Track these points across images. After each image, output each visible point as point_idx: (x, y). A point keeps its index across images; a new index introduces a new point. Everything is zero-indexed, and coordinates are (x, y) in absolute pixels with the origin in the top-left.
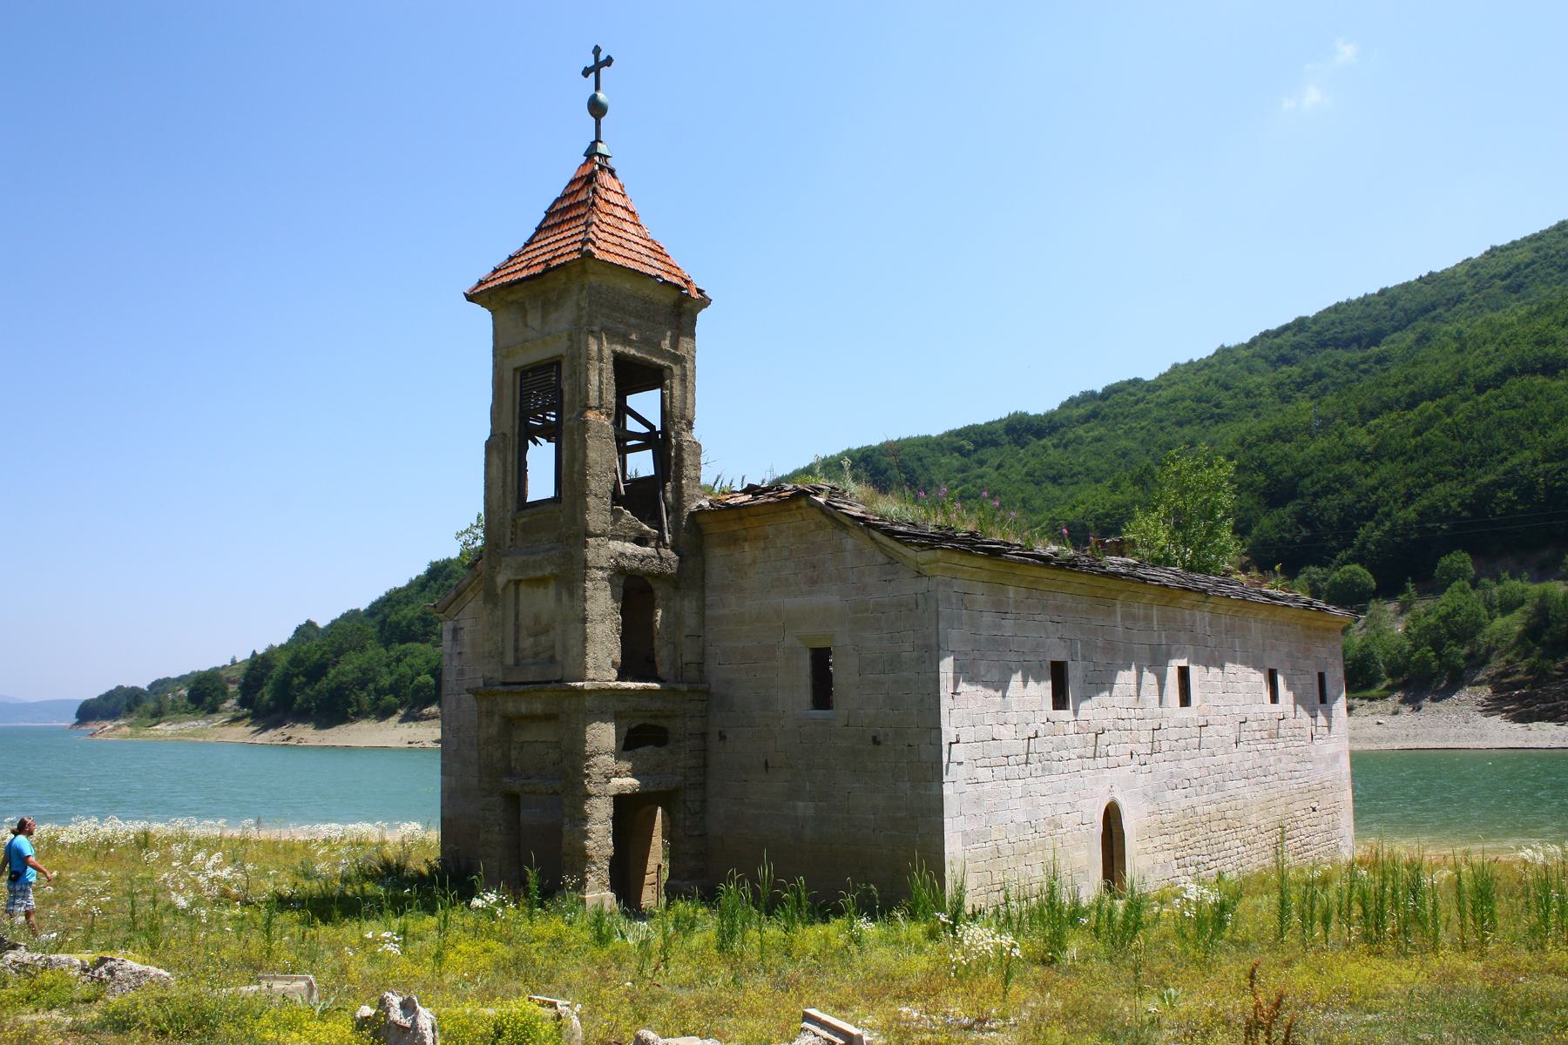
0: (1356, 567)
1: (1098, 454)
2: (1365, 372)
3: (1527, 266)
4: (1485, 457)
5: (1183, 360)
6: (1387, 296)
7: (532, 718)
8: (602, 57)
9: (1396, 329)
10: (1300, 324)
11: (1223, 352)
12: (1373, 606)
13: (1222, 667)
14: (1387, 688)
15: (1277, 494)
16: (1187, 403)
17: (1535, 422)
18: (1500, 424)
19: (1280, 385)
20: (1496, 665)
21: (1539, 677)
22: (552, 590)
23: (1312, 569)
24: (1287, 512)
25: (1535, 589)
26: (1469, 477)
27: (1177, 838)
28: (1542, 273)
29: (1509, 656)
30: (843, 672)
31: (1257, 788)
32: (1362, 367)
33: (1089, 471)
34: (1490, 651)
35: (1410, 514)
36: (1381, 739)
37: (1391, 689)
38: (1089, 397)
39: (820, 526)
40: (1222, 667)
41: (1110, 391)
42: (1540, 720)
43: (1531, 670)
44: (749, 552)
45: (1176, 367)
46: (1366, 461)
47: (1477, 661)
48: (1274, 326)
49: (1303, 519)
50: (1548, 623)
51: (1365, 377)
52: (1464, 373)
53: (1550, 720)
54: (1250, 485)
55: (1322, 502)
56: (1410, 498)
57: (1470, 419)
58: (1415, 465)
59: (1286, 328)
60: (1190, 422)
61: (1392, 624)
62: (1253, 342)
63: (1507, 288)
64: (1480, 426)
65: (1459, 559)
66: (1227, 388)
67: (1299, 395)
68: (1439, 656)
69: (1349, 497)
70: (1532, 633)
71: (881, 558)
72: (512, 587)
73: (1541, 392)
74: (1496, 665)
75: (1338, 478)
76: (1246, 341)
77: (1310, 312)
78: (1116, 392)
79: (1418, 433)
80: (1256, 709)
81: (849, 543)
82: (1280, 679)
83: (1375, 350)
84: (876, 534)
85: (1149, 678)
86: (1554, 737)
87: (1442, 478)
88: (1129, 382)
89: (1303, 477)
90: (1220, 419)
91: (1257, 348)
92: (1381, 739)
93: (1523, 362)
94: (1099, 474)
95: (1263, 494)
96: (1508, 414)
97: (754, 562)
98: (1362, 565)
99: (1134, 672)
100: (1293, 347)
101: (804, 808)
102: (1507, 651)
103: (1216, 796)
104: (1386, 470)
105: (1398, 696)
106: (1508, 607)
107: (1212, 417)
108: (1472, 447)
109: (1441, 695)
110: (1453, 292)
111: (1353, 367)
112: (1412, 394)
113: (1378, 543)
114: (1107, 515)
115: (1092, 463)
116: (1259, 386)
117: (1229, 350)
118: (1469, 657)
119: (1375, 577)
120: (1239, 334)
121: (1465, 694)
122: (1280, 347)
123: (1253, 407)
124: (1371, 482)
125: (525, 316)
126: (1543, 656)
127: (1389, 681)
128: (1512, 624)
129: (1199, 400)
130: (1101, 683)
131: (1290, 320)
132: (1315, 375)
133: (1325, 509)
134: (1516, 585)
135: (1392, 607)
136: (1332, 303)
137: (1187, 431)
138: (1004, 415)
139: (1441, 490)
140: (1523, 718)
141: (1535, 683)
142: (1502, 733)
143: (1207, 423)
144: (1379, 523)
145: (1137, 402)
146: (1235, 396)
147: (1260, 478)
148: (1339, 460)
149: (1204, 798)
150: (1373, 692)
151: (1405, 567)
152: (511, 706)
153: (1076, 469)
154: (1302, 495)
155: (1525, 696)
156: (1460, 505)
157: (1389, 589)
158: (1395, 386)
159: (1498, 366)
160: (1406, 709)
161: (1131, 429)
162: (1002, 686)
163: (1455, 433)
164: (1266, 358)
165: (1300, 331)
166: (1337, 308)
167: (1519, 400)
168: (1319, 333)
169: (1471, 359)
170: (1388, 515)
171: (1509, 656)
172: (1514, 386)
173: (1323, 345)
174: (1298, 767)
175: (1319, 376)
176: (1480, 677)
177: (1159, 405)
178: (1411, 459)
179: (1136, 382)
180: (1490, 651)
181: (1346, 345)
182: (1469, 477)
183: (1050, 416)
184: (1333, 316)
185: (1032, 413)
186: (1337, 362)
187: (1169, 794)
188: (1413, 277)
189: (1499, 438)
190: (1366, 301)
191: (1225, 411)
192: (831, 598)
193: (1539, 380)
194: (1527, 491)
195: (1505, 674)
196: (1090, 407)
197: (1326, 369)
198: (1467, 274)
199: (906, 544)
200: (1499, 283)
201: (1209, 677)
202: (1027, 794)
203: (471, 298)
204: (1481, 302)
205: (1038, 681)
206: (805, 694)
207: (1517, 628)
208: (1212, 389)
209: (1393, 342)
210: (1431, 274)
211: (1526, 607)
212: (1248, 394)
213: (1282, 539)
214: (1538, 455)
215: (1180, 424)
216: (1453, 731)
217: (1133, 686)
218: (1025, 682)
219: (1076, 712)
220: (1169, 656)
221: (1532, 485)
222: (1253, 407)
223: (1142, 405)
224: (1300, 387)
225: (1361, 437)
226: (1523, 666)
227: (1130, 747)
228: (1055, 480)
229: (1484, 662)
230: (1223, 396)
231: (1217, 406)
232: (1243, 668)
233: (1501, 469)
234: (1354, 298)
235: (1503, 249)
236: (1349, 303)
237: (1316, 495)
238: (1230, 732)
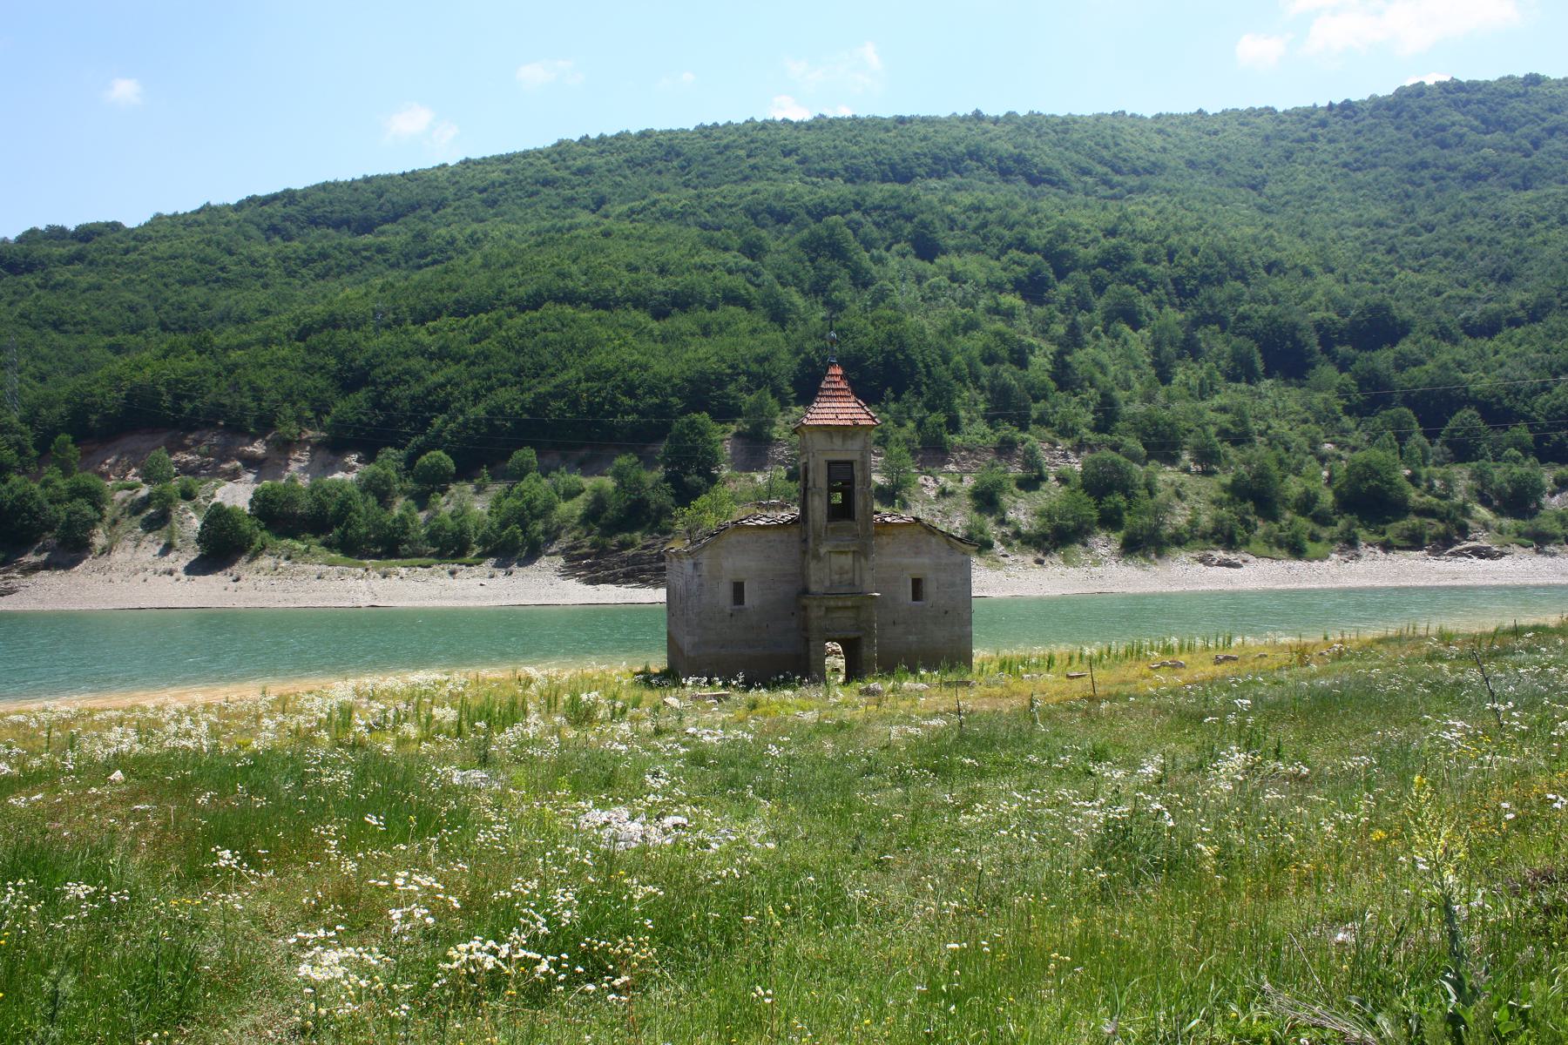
0: (440, 453)
1: (100, 304)
2: (369, 259)
3: (502, 184)
4: (539, 370)
5: (168, 211)
6: (376, 186)
7: (838, 608)
9: (385, 221)
10: (289, 196)
12: (453, 488)
14: (479, 556)
15: (351, 380)
16: (190, 262)
17: (573, 346)
18: (546, 345)
19: (286, 259)
20: (565, 540)
21: (601, 551)
22: (850, 556)
23: (390, 450)
24: (361, 395)
25: (589, 483)
26: (526, 385)
28: (513, 195)
29: (576, 533)
30: (930, 588)
32: (365, 254)
33: (95, 322)
34: (560, 528)
35: (478, 411)
36: (487, 598)
37: (483, 556)
38: (57, 234)
41: (87, 234)
42: (604, 582)
43: (594, 545)
44: (885, 539)
45: (159, 218)
46: (431, 359)
47: (552, 535)
48: (262, 192)
49: (376, 404)
50: (605, 509)
51: (368, 264)
52: (501, 291)
53: (612, 582)
54: (322, 368)
55: (394, 392)
56: (477, 396)
57: (521, 336)
58: (476, 370)
59: (274, 198)
60: (194, 282)
61: (474, 503)
62: (239, 206)
63: (484, 201)
64: (529, 343)
65: (527, 454)
66: (231, 253)
67: (304, 271)
68: (524, 533)
69: (417, 389)
70: (593, 515)
73: (573, 321)
74: (565, 540)
75: (407, 372)
76: (233, 202)
77: (298, 184)
78: (100, 234)
79: (474, 341)
81: (934, 540)
83: (368, 239)
86: (617, 596)
87: (504, 384)
88: (107, 225)
89: (373, 367)
90: (228, 283)
91: (246, 213)
92: (487, 598)
93: (549, 290)
94: (109, 327)
95: (334, 377)
96: (552, 336)
98: (447, 452)
100: (285, 218)
101: (911, 638)
102: (573, 529)
104: (451, 370)
105: (493, 560)
106: (570, 495)
107: (217, 280)
108: (526, 361)
109: (524, 562)
110: (435, 195)
111: (356, 252)
112: (457, 302)
113: (452, 433)
114: (178, 381)
115: (96, 313)
116: (266, 256)
117: (215, 209)
118: (546, 532)
119: (456, 464)
120: (228, 194)
121: (544, 561)
122: (271, 216)
123: (260, 276)
124: (439, 378)
126: (601, 535)
127: (478, 550)
128: (577, 506)
129: (203, 261)
131: (279, 189)
132: (320, 254)
133: (398, 399)
134: (576, 478)
135: (470, 488)
136: (320, 180)
137: (198, 292)
139: (503, 395)
140: (593, 582)
141: (598, 556)
142: (577, 593)
143: (215, 286)
144: (453, 418)
145: (127, 252)
146: (239, 263)
147: (332, 362)
148: (406, 356)
150: (467, 559)
151: (481, 455)
152: (832, 603)
153: (81, 317)
154: (374, 383)
155: (591, 565)
156: (522, 407)
157: (465, 473)
158: (441, 291)
159: (531, 288)
160: (500, 573)
161: (131, 281)
163: (506, 342)
164: (258, 226)
165: (290, 203)
166: (324, 187)
167: (558, 325)
168: (309, 209)
169: (505, 279)
170: (461, 411)
171: (576, 533)
172: (550, 310)
173: (314, 222)
175: (324, 256)
176: (554, 549)
177: (156, 259)
178: (473, 363)
179: (115, 227)
180: (560, 528)
181: (337, 225)
182: (526, 385)
184: (322, 195)
186: (340, 245)
188: (397, 171)
189: (547, 355)
190: (352, 185)
191: (230, 276)
192: (925, 560)
193: (569, 310)
194: (574, 404)
195: (574, 548)
196: (74, 247)
197: (330, 251)
198: (448, 180)
200: (476, 194)
204: (463, 210)
206: (910, 596)
207: (578, 512)
208: (211, 252)
209: (383, 233)
210: (413, 172)
211: (582, 496)
212: (253, 263)
213: (359, 420)
214: (582, 375)
215: (184, 283)
216: (543, 591)
221: (578, 398)
222: (260, 276)
223: (133, 256)
224: (305, 263)
225: (422, 335)
226: (587, 542)
228: (57, 326)
229: (556, 538)
230: (226, 260)
231: (222, 269)
233: (554, 382)
234: (341, 179)
235: (476, 163)
236: (336, 184)
237: (388, 385)
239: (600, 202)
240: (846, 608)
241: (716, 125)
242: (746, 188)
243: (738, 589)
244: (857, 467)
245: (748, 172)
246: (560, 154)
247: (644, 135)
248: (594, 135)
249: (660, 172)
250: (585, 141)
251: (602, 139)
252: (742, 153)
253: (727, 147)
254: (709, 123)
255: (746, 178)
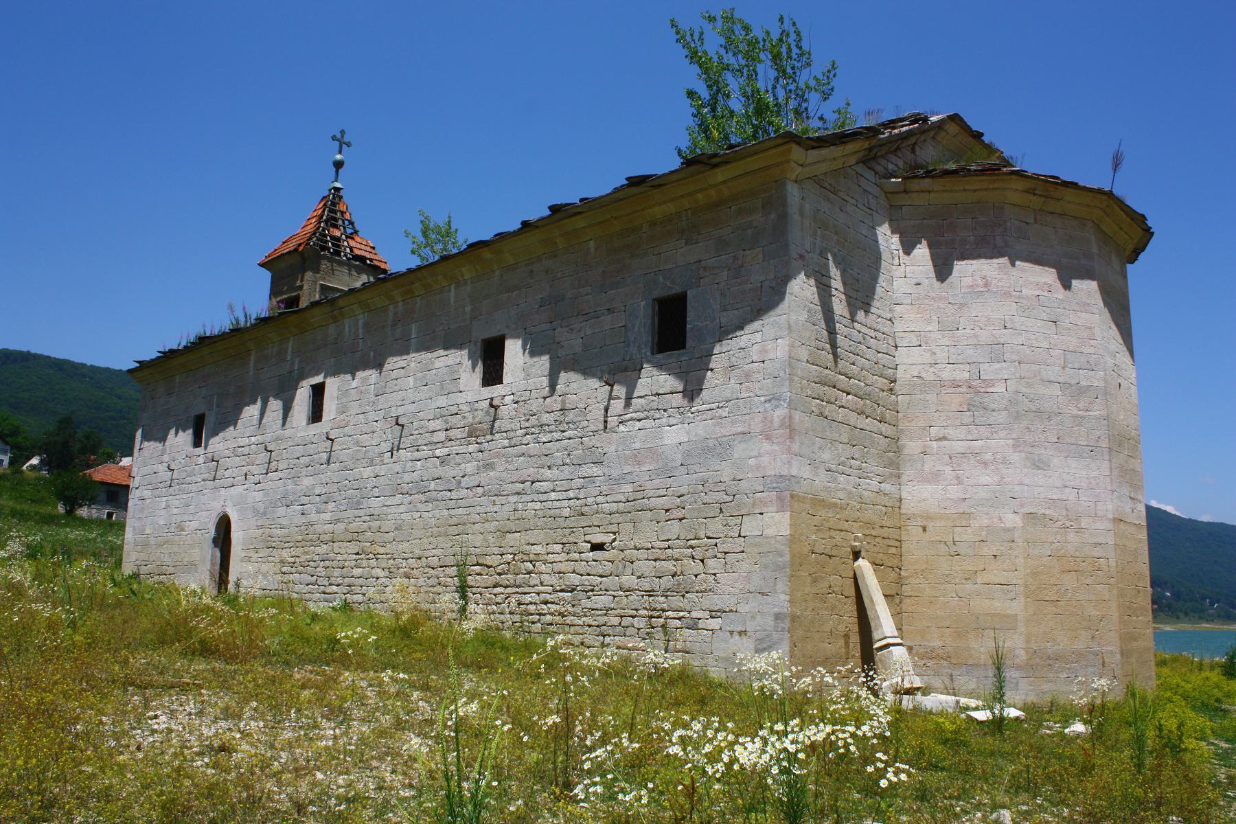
8: (339, 136)
13: (379, 366)
27: (285, 554)
31: (421, 507)
40: (379, 366)
80: (442, 401)
82: (514, 350)
85: (275, 405)
99: (259, 403)
103: (350, 514)
130: (229, 419)
149: (327, 516)
162: (163, 439)
174: (548, 474)
187: (281, 511)
201: (354, 384)
202: (167, 506)
205: (184, 431)
217: (257, 417)
218: (177, 433)
219: (206, 448)
220: (303, 377)
227: (245, 469)
232: (425, 356)
238: (382, 438)
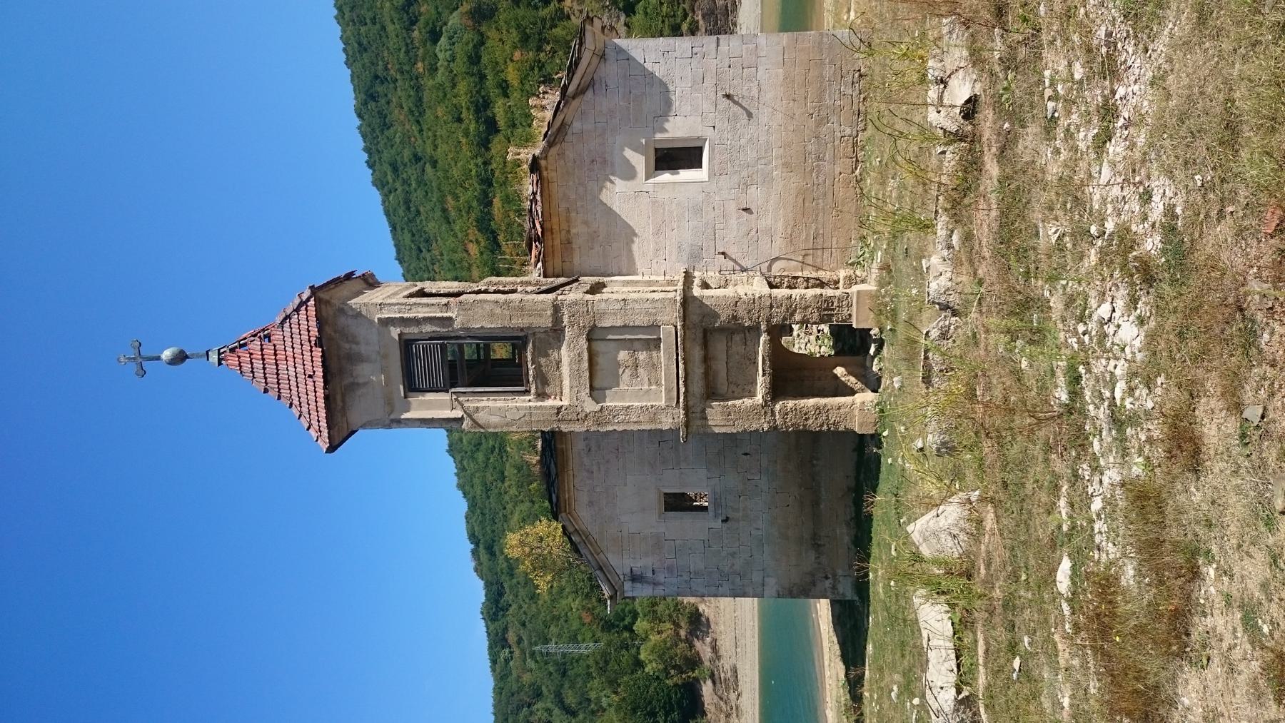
3: (413, 235)
11: (452, 450)
39: (561, 155)
44: (578, 229)
71: (589, 93)
72: (595, 393)
81: (577, 126)
84: (571, 89)
97: (586, 223)
125: (358, 384)
138: (482, 623)
183: (488, 585)
185: (483, 599)
199: (580, 58)
203: (332, 449)
235: (398, 252)
239: (417, 158)
240: (706, 359)
241: (344, 50)
242: (390, 28)
243: (677, 503)
244: (413, 330)
245: (378, 26)
246: (383, 186)
247: (360, 116)
248: (365, 156)
249: (388, 103)
250: (371, 165)
251: (367, 150)
252: (363, 29)
253: (360, 44)
254: (344, 56)
255: (384, 28)
